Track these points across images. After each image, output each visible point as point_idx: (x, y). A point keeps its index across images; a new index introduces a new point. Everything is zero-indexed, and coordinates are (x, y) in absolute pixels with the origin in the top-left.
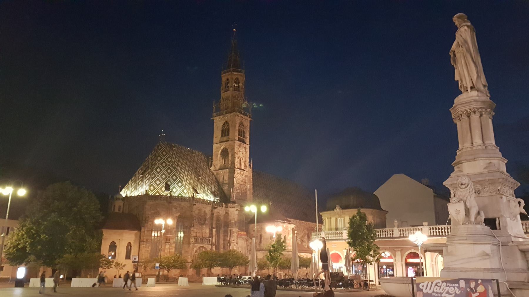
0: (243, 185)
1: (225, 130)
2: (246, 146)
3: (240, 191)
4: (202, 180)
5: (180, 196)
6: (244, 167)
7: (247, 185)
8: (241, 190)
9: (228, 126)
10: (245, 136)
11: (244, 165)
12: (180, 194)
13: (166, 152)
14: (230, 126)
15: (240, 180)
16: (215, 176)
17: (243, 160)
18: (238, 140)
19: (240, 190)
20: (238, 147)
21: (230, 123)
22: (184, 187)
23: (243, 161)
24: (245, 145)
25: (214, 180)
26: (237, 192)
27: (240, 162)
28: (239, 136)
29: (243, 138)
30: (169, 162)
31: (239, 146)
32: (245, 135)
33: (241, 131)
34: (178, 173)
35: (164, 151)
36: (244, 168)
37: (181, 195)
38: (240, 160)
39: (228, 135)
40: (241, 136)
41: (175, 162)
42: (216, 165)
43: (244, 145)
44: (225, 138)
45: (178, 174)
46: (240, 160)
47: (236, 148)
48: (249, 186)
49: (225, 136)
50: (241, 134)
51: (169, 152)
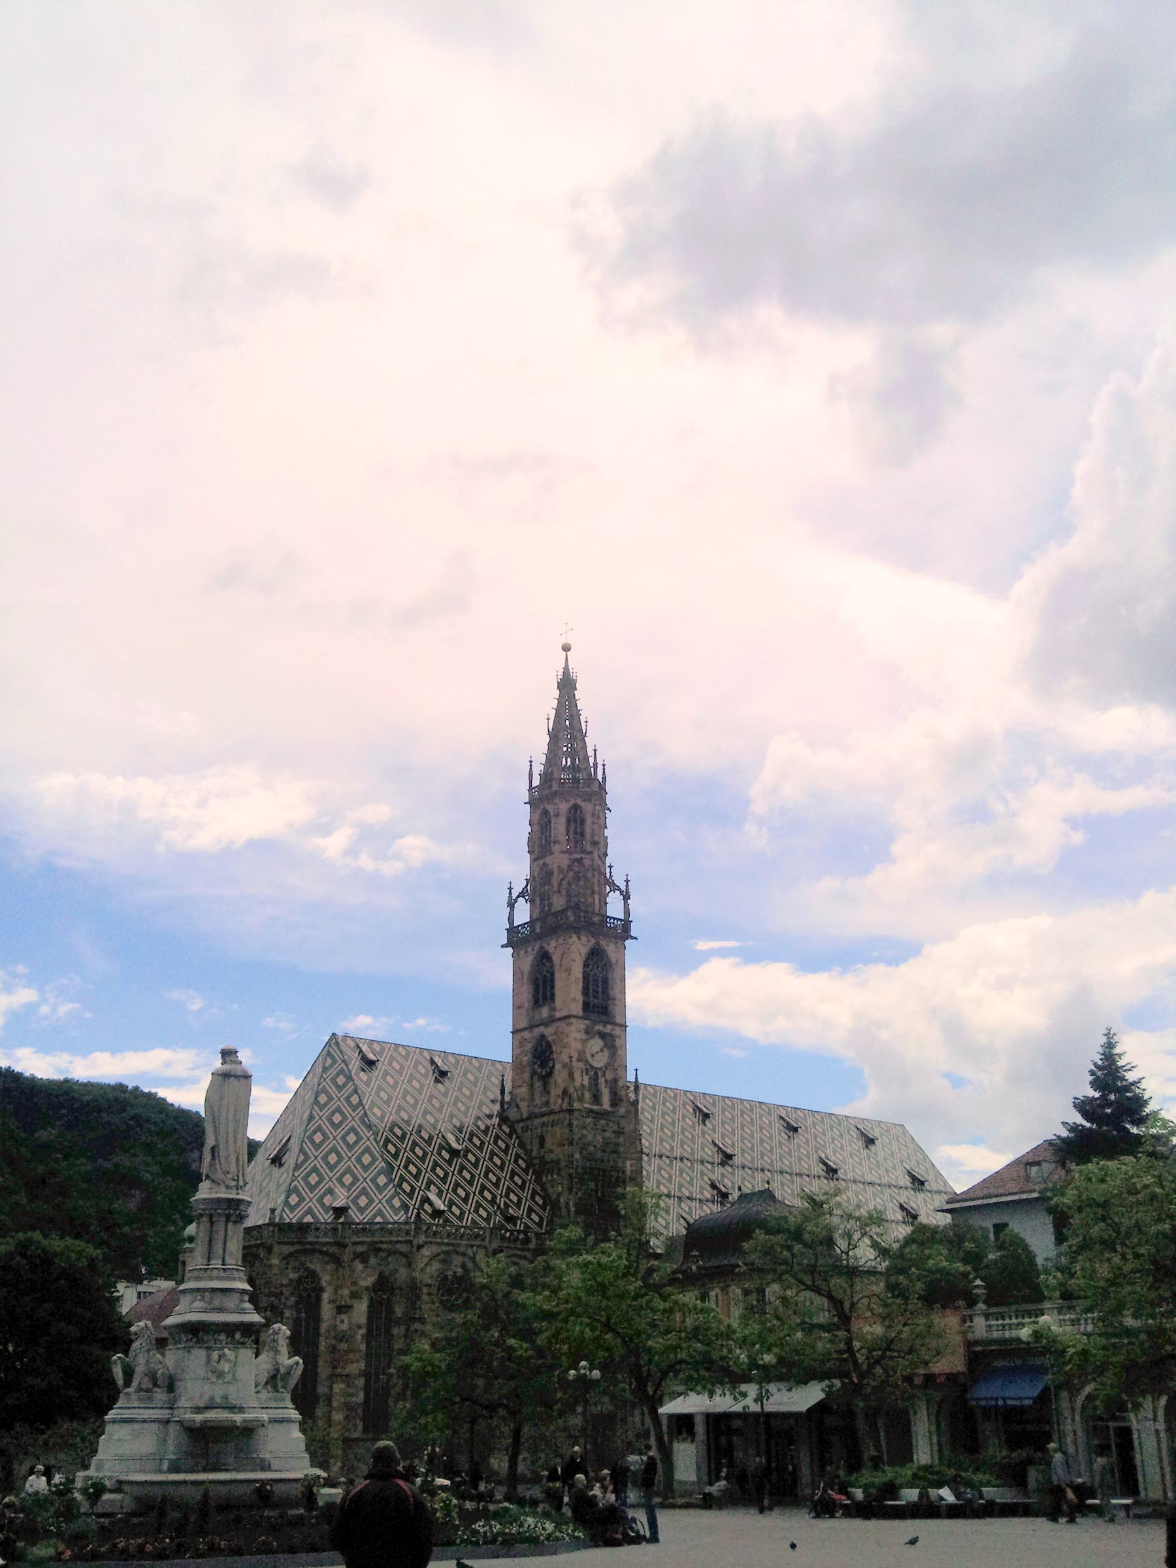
1: (545, 983)
2: (613, 1029)
3: (596, 1185)
4: (465, 1156)
5: (379, 1219)
6: (611, 1100)
7: (624, 1162)
9: (552, 966)
10: (611, 997)
11: (611, 1092)
12: (380, 1213)
14: (557, 967)
17: (604, 1075)
18: (581, 1014)
19: (596, 1181)
20: (584, 1037)
21: (556, 958)
23: (606, 1081)
24: (609, 1027)
27: (596, 1085)
30: (354, 1108)
31: (587, 1032)
32: (610, 992)
34: (377, 1143)
35: (341, 1072)
36: (612, 1106)
37: (383, 1216)
38: (595, 1080)
42: (521, 1100)
43: (605, 1026)
44: (545, 1012)
46: (595, 1080)
47: (575, 1039)
49: (545, 999)
51: (357, 1074)
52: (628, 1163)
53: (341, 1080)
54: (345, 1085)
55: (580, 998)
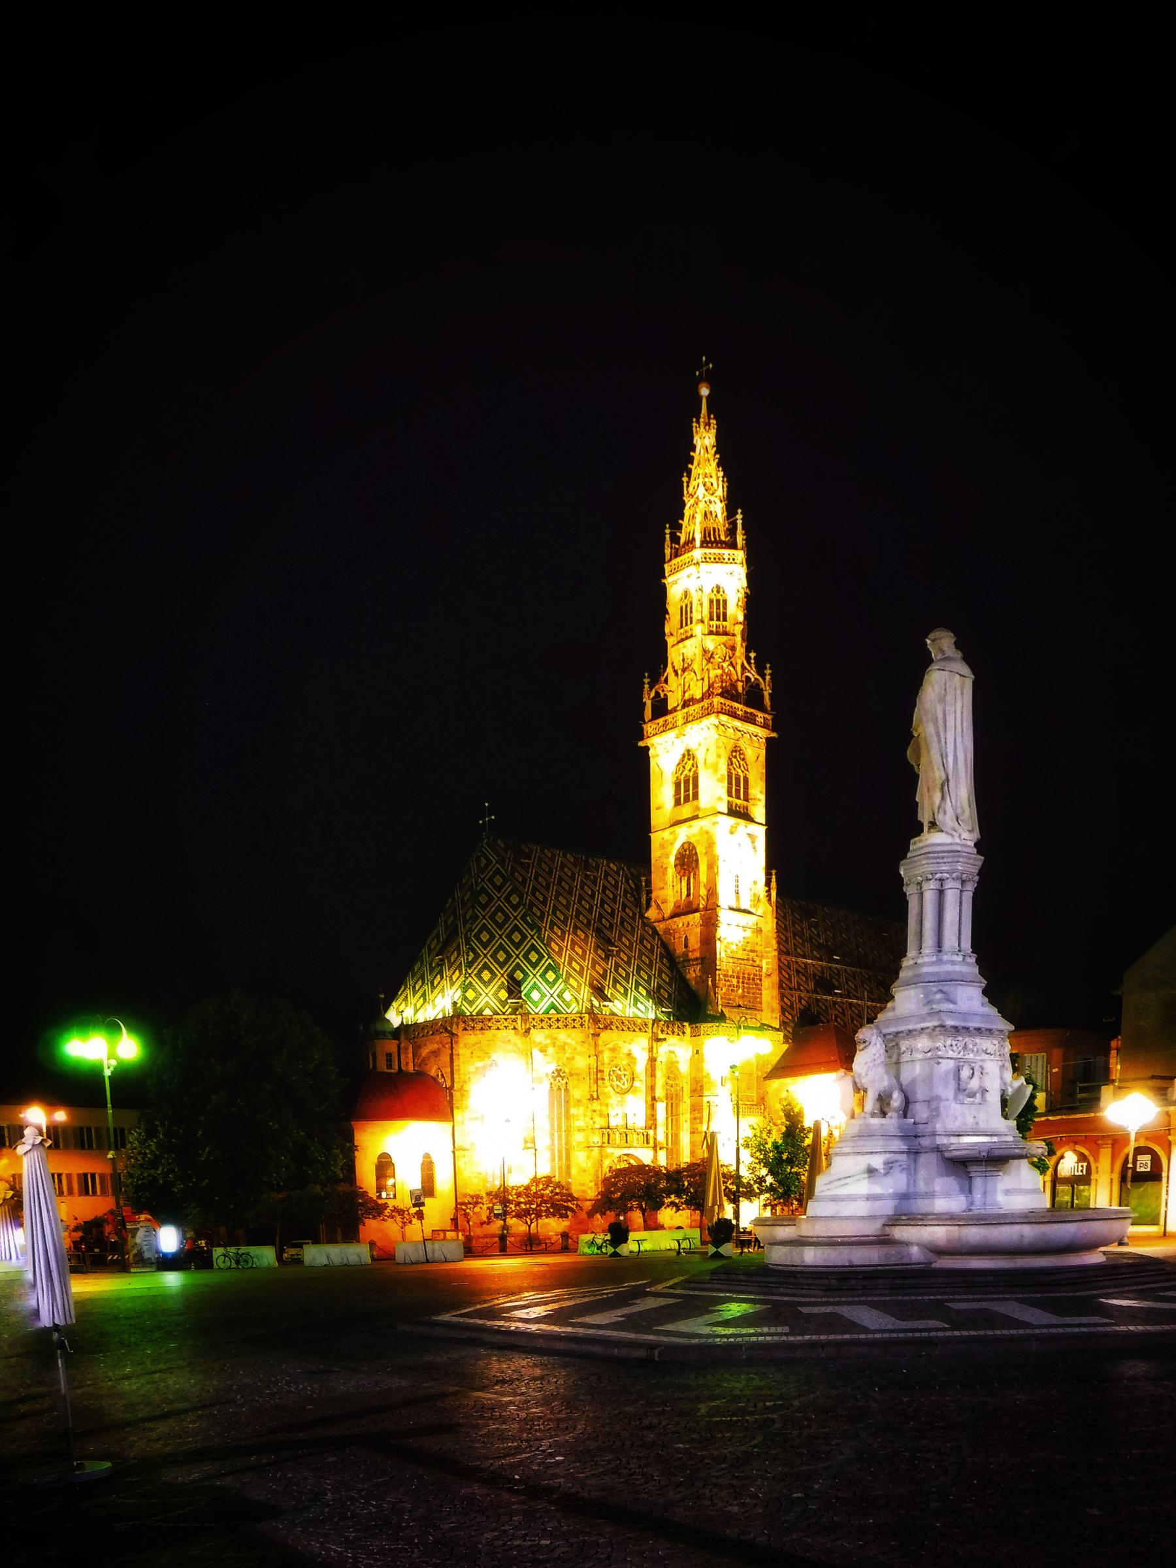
0: (748, 960)
1: (687, 782)
3: (738, 982)
7: (761, 961)
8: (741, 975)
9: (695, 765)
13: (502, 876)
15: (737, 945)
16: (660, 939)
19: (738, 977)
22: (563, 984)
25: (658, 951)
26: (728, 983)
28: (731, 799)
29: (745, 803)
33: (738, 779)
34: (542, 941)
35: (498, 872)
39: (696, 796)
40: (738, 797)
41: (532, 904)
44: (686, 811)
45: (544, 944)
48: (767, 963)
49: (687, 799)
50: (738, 791)
52: (764, 962)
53: (498, 880)
54: (503, 885)
55: (726, 798)
